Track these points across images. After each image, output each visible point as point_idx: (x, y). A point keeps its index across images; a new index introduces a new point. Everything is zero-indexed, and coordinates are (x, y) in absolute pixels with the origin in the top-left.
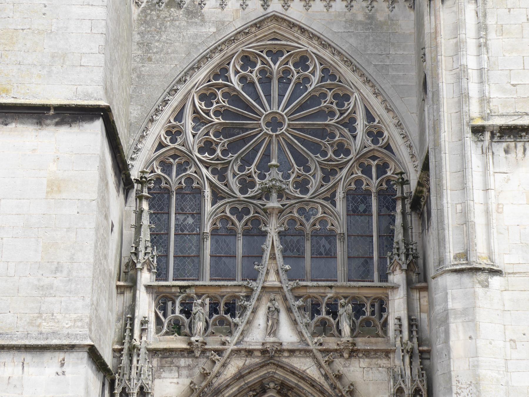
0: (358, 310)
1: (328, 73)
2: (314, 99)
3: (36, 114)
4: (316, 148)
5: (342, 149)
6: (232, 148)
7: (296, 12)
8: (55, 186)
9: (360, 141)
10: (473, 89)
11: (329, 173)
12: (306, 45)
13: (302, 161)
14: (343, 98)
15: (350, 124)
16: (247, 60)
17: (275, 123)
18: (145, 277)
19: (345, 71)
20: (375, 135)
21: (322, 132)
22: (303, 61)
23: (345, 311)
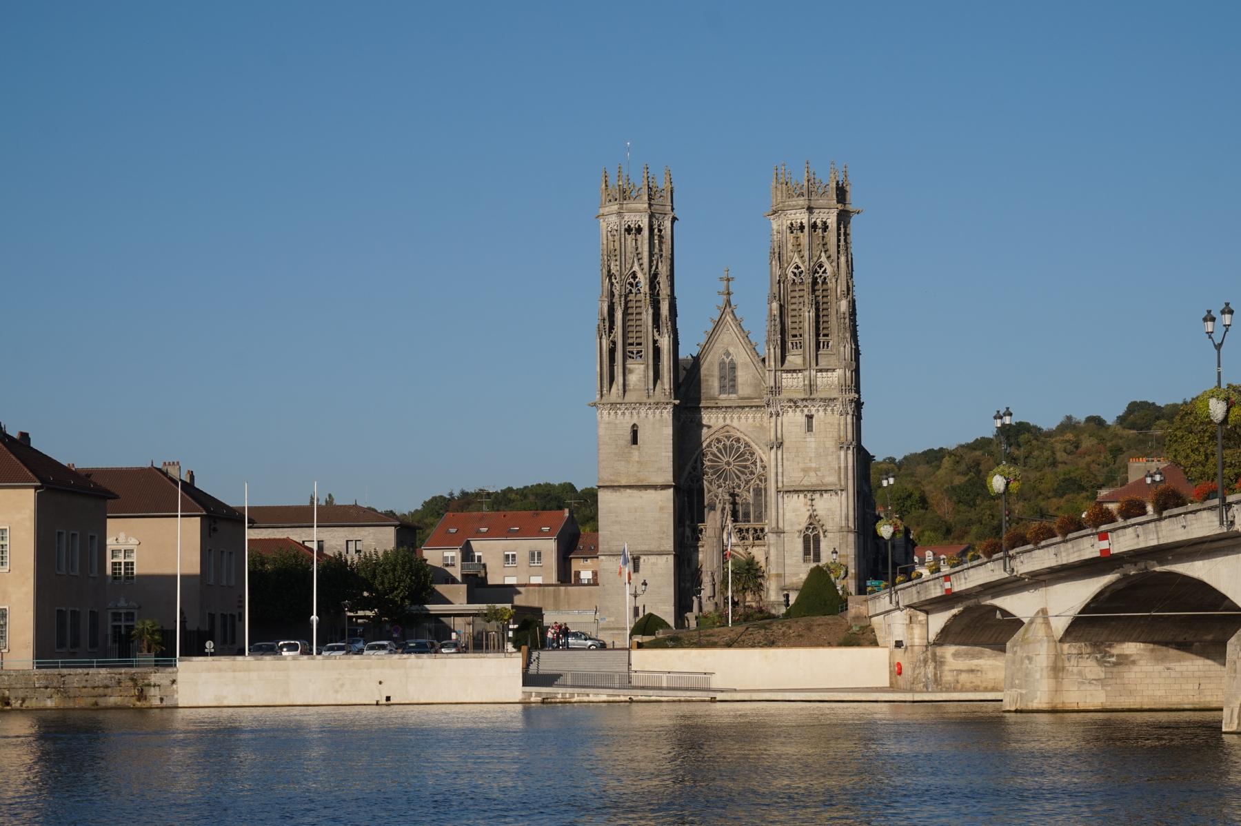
0: (756, 530)
1: (747, 445)
2: (742, 455)
3: (655, 487)
4: (743, 473)
5: (752, 473)
6: (715, 473)
7: (735, 423)
8: (661, 509)
9: (759, 469)
10: (780, 478)
11: (747, 482)
12: (738, 435)
13: (738, 477)
14: (752, 454)
15: (755, 463)
16: (719, 441)
17: (728, 463)
18: (688, 522)
19: (752, 444)
20: (764, 467)
21: (745, 467)
22: (738, 440)
23: (751, 532)
